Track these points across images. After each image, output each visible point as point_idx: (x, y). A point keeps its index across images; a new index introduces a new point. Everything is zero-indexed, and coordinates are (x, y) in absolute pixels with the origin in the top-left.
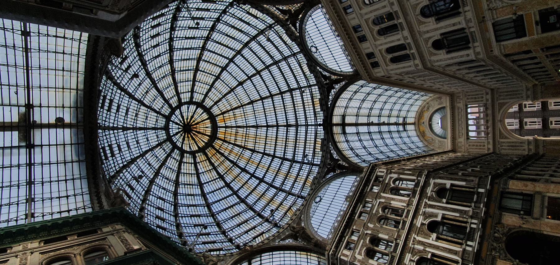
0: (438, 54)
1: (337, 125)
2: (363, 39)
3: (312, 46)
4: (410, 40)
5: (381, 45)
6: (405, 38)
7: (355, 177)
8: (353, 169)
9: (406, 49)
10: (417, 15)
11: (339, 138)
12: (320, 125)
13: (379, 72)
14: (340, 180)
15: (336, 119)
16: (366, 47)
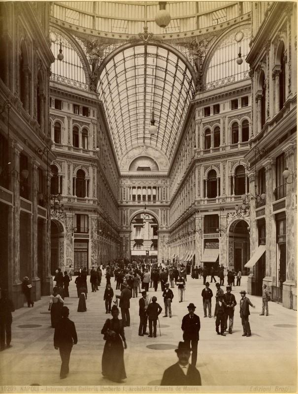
0: (205, 173)
1: (146, 50)
2: (234, 105)
3: (243, 36)
4: (221, 152)
5: (224, 123)
6: (224, 148)
7: (85, 82)
8: (93, 80)
9: (215, 147)
10: (239, 162)
11: (129, 52)
12: (146, 29)
13: (199, 115)
14: (80, 64)
15: (152, 50)
16: (226, 107)
